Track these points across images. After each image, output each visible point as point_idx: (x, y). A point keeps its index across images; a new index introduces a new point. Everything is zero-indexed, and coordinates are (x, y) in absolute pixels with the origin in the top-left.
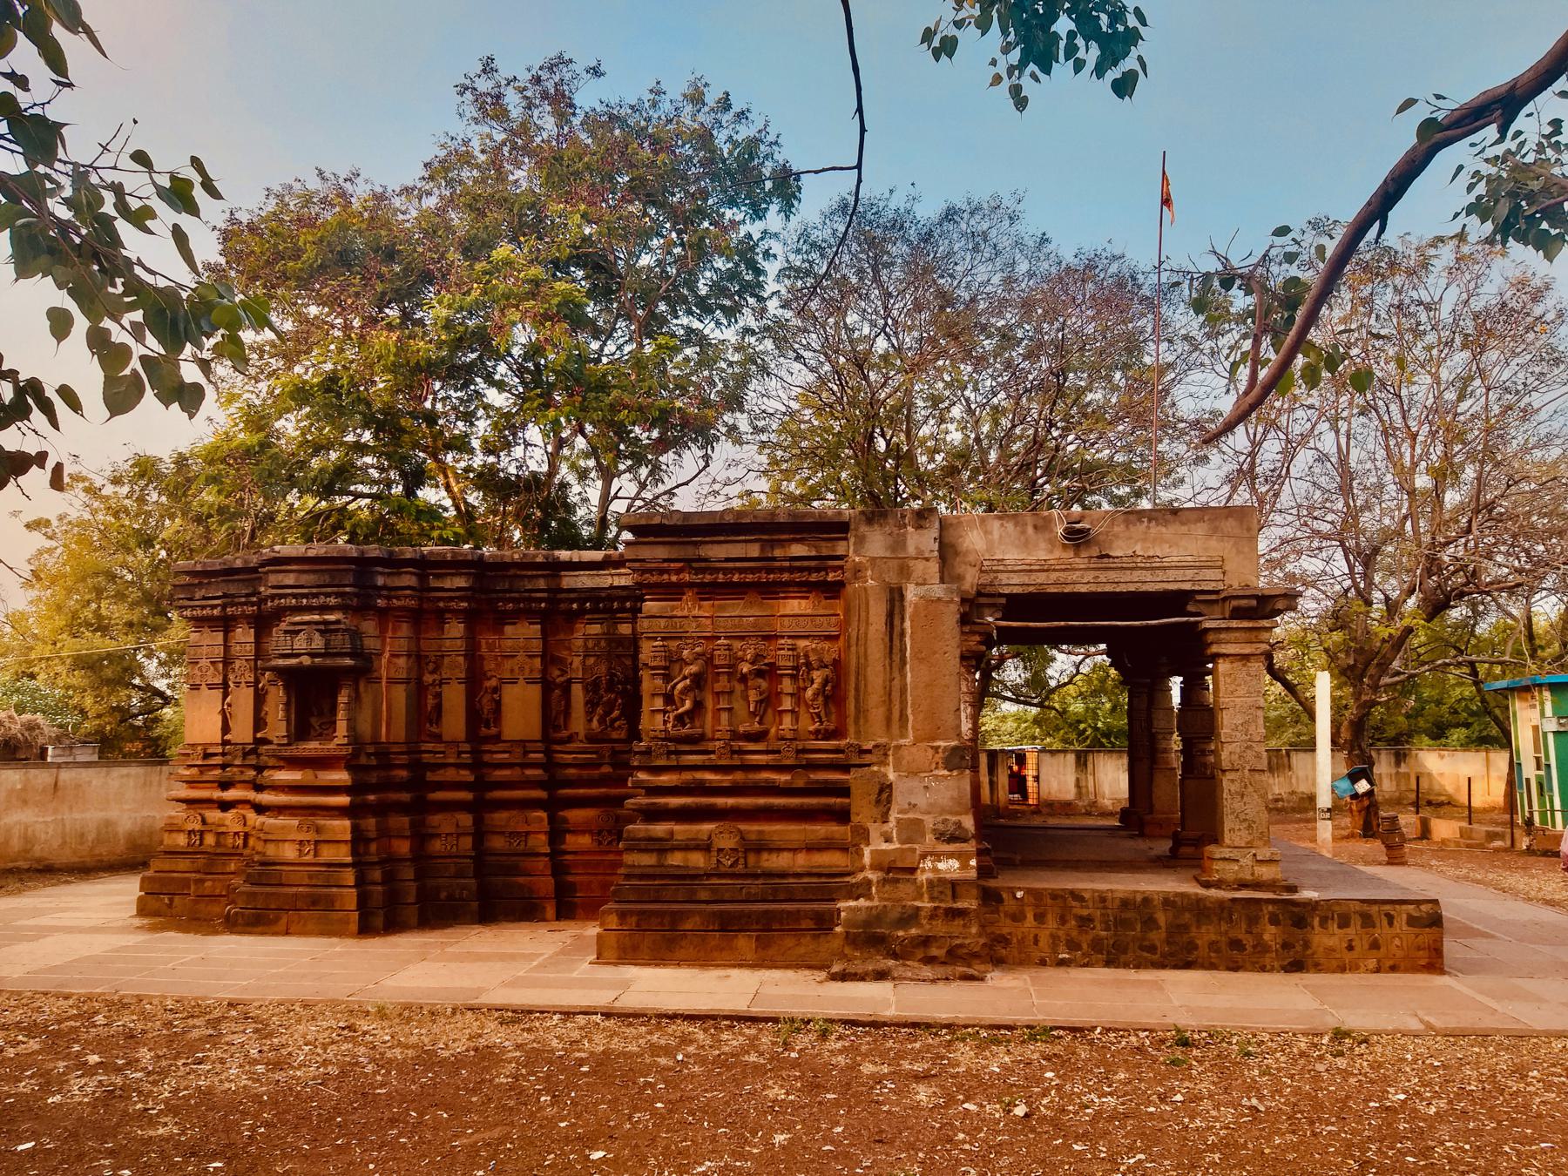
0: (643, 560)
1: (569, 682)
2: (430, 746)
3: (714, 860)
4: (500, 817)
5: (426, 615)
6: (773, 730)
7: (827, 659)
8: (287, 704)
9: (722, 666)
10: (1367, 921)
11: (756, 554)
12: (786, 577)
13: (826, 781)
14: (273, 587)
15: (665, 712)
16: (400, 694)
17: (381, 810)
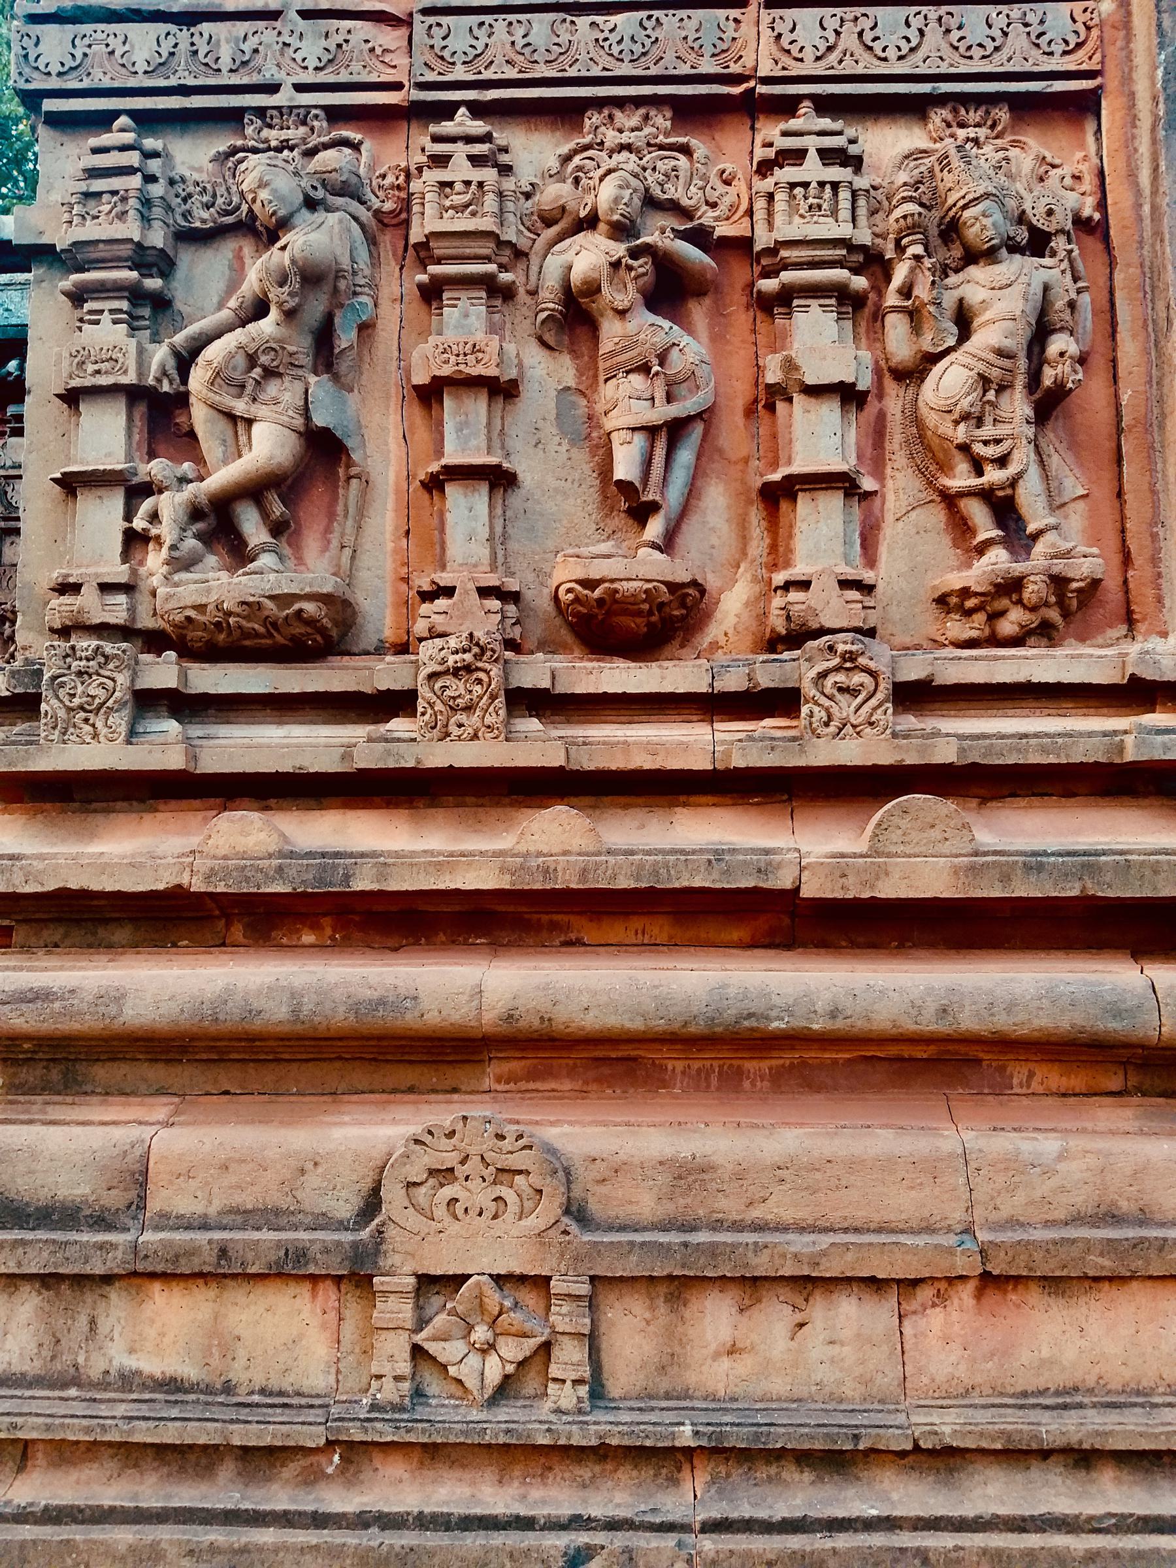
3: (393, 1353)
13: (1087, 862)
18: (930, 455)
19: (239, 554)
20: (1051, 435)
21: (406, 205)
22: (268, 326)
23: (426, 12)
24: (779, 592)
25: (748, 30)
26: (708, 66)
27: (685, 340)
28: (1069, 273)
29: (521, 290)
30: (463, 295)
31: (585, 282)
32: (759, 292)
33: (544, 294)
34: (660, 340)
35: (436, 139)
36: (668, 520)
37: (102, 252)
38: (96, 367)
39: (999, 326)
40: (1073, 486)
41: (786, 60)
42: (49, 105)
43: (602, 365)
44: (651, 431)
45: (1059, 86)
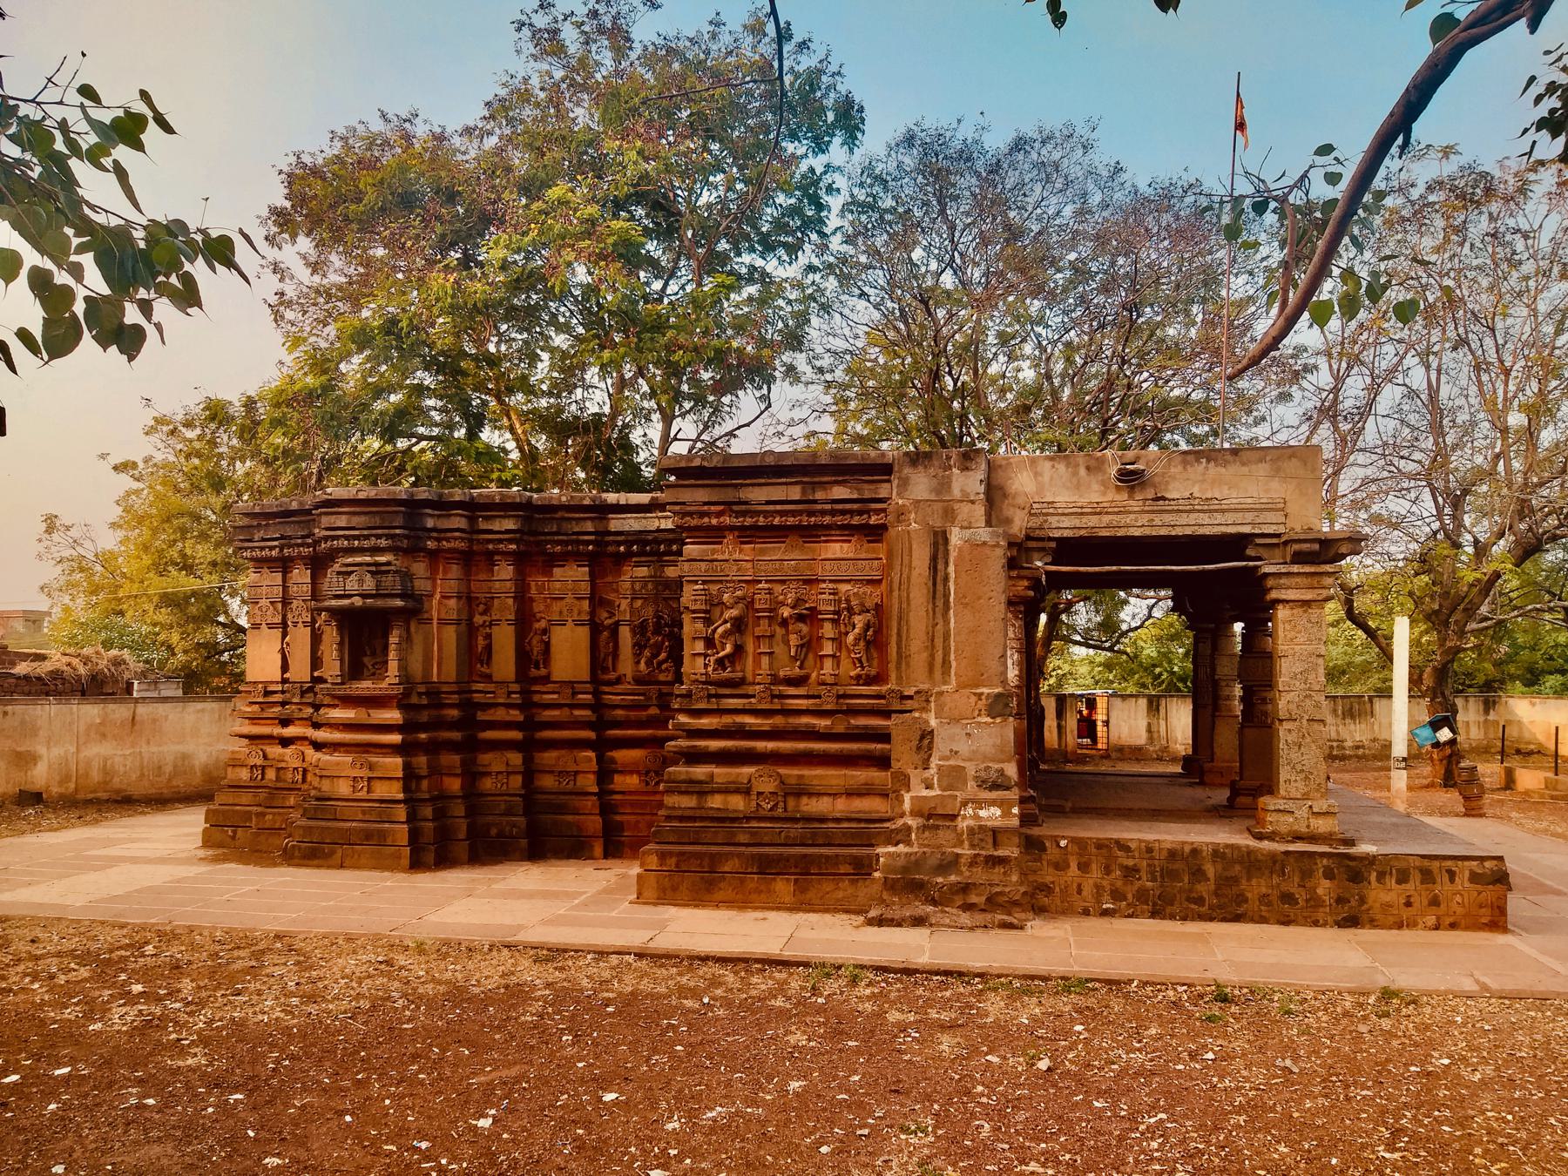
1: (617, 624)
2: (480, 686)
3: (754, 804)
4: (549, 757)
5: (475, 558)
6: (814, 675)
7: (869, 604)
8: (341, 644)
9: (764, 610)
10: (1427, 876)
11: (797, 497)
12: (827, 520)
13: (866, 727)
14: (327, 529)
15: (706, 656)
16: (450, 633)
17: (433, 748)
19: (724, 669)
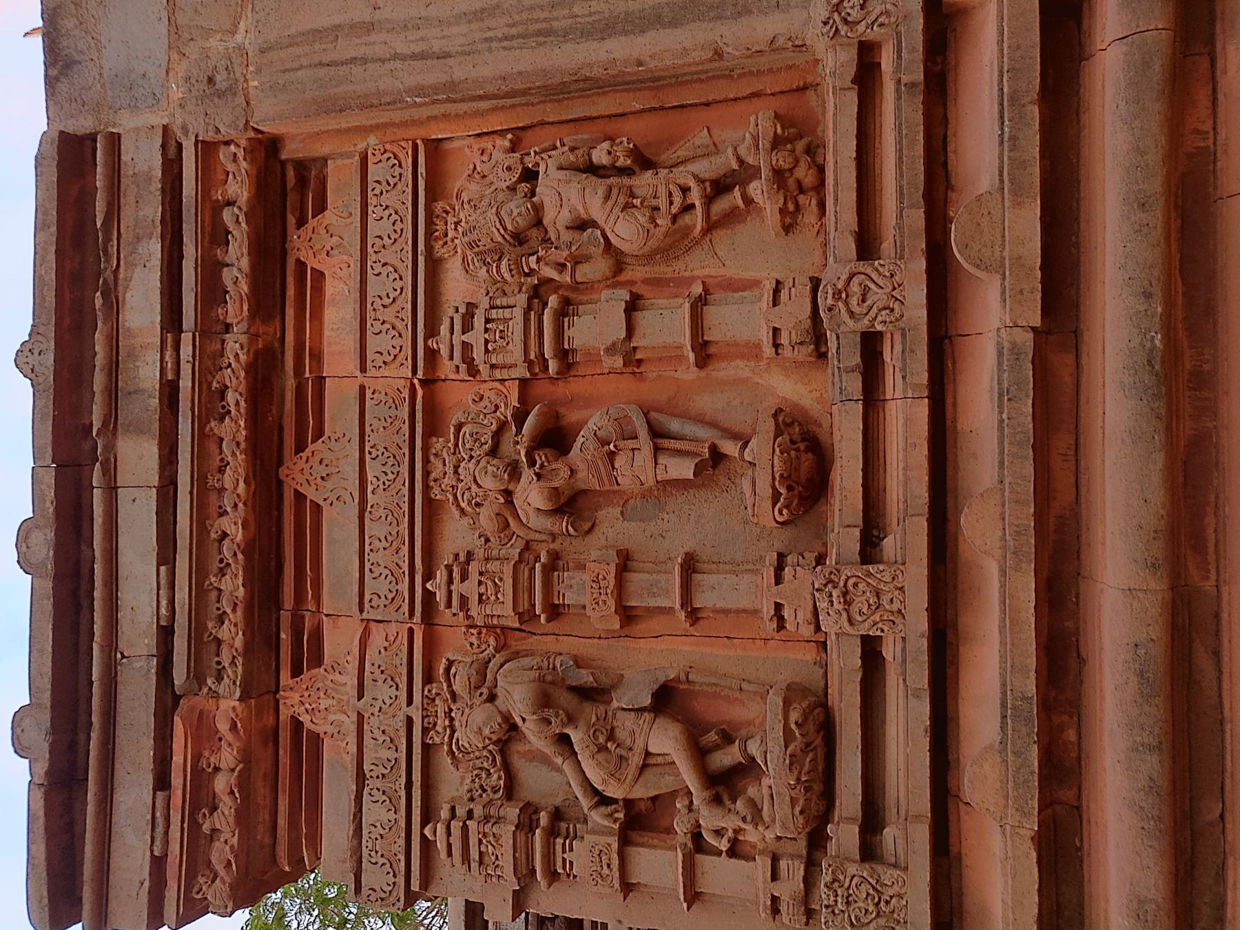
0: (158, 864)
18: (677, 243)
19: (749, 769)
20: (663, 157)
21: (490, 628)
22: (576, 736)
23: (361, 611)
24: (780, 351)
25: (380, 385)
26: (404, 412)
27: (590, 424)
28: (553, 152)
29: (552, 546)
30: (556, 588)
31: (550, 500)
32: (557, 373)
33: (556, 529)
34: (591, 445)
35: (449, 605)
36: (722, 437)
37: (521, 856)
38: (605, 867)
39: (589, 198)
40: (702, 138)
41: (400, 358)
42: (415, 887)
43: (607, 487)
44: (657, 450)
45: (422, 169)
